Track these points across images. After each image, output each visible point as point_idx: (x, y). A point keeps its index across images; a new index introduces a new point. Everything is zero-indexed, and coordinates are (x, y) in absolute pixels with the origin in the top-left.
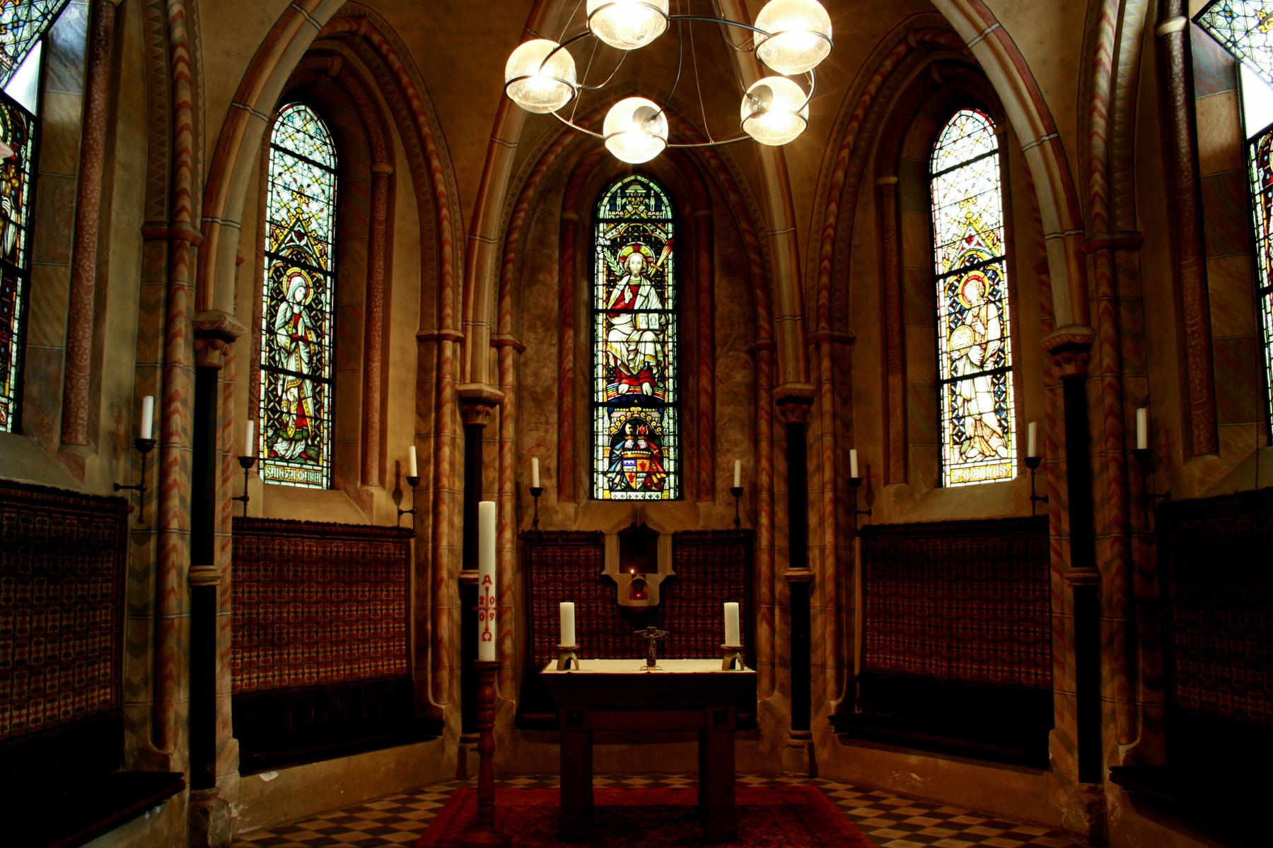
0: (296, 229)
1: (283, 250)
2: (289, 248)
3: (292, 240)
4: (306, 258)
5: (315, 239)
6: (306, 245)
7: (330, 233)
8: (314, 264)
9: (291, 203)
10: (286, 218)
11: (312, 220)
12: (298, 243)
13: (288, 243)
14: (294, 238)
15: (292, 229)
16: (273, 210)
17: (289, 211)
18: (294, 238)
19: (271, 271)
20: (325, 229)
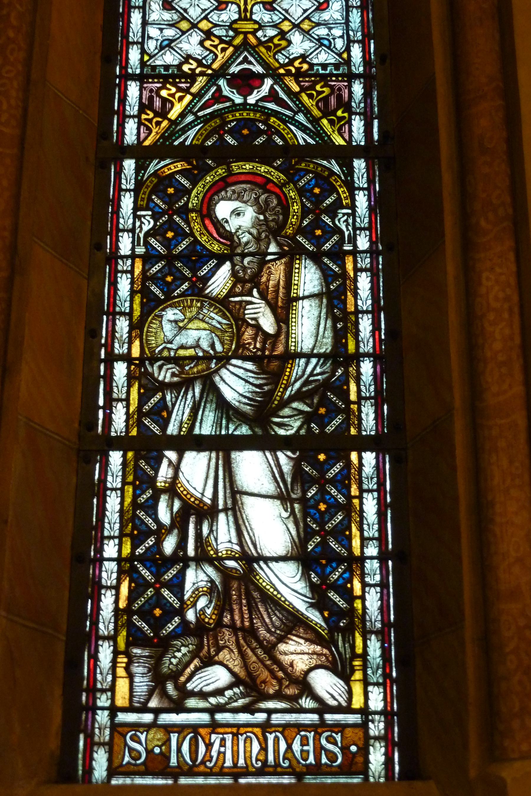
0: (235, 69)
1: (185, 130)
2: (206, 120)
3: (219, 97)
4: (271, 131)
5: (298, 75)
6: (272, 96)
7: (356, 52)
8: (301, 138)
9: (214, 17)
10: (196, 51)
11: (296, 37)
12: (238, 99)
13: (200, 109)
14: (226, 91)
15: (222, 72)
16: (151, 46)
17: (208, 34)
18: (226, 91)
19: (145, 191)
20: (340, 44)
